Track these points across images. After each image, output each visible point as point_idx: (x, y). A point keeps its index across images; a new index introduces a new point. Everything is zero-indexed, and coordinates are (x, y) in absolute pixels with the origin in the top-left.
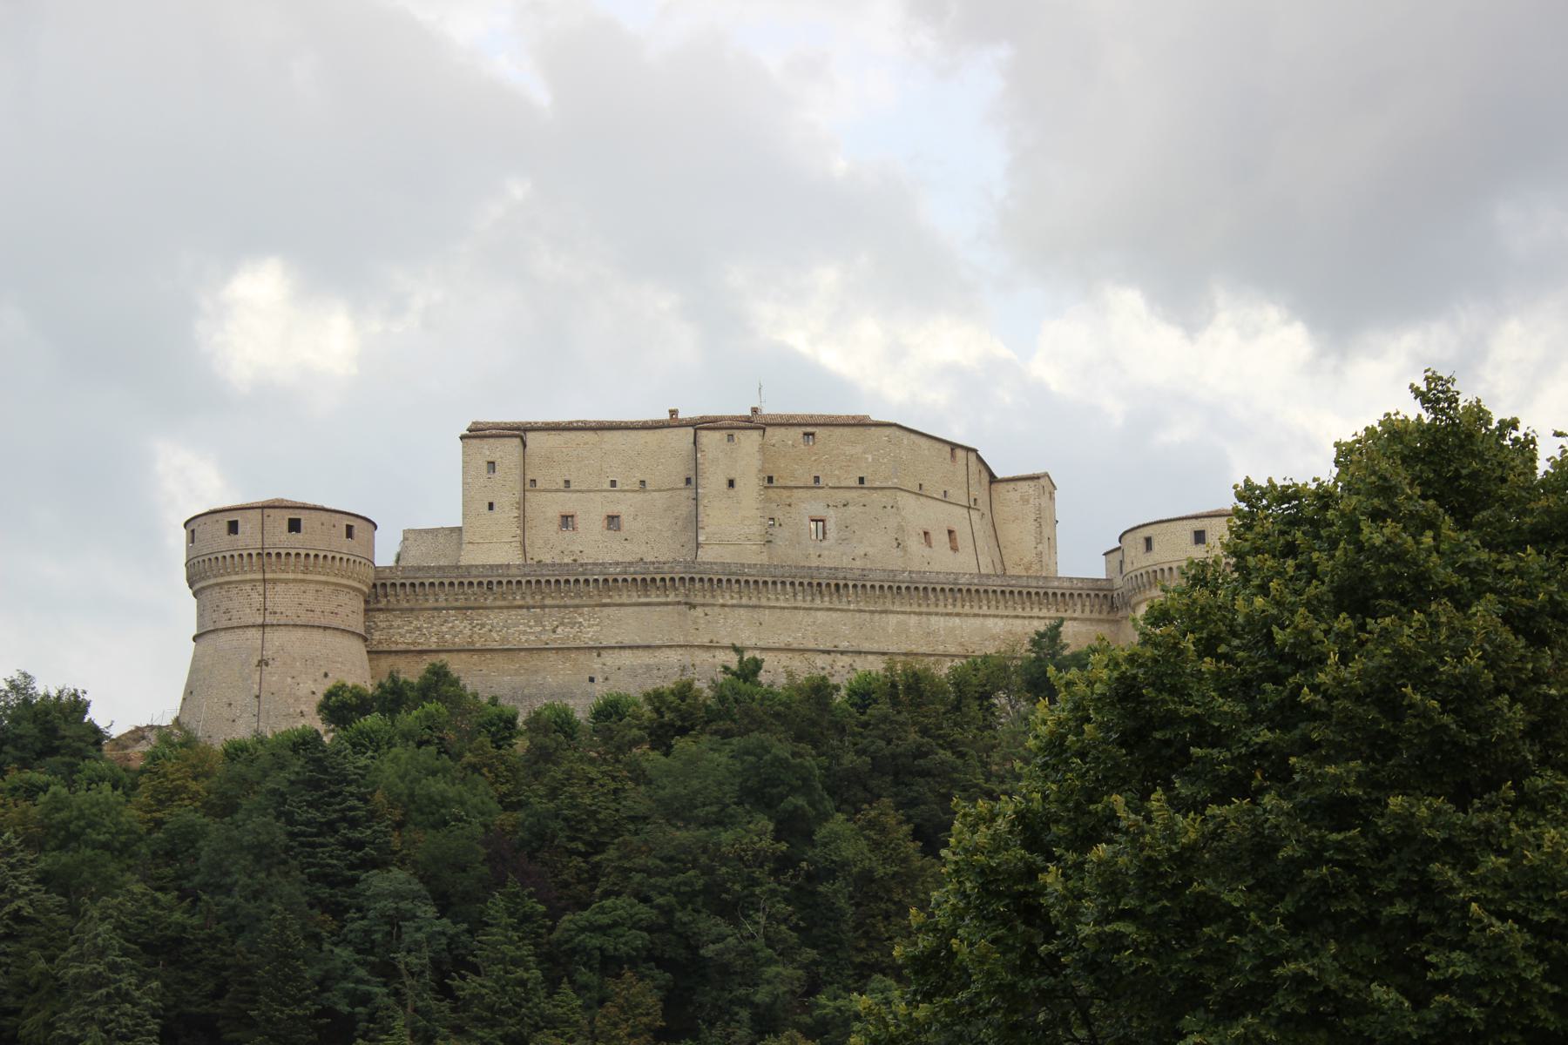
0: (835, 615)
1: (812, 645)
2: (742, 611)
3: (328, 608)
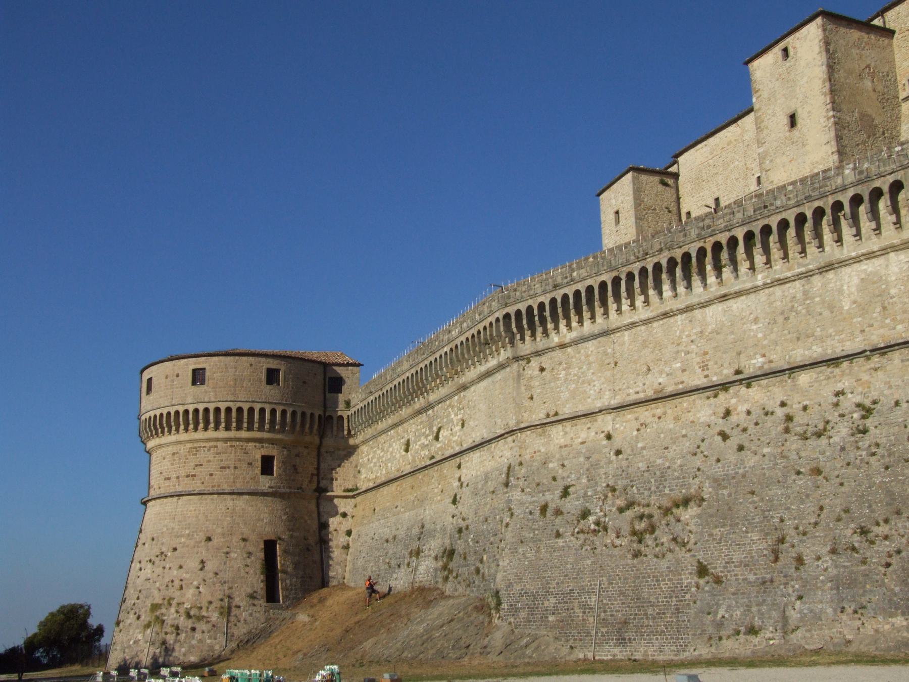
0: (735, 305)
1: (699, 380)
2: (591, 346)
3: (183, 473)
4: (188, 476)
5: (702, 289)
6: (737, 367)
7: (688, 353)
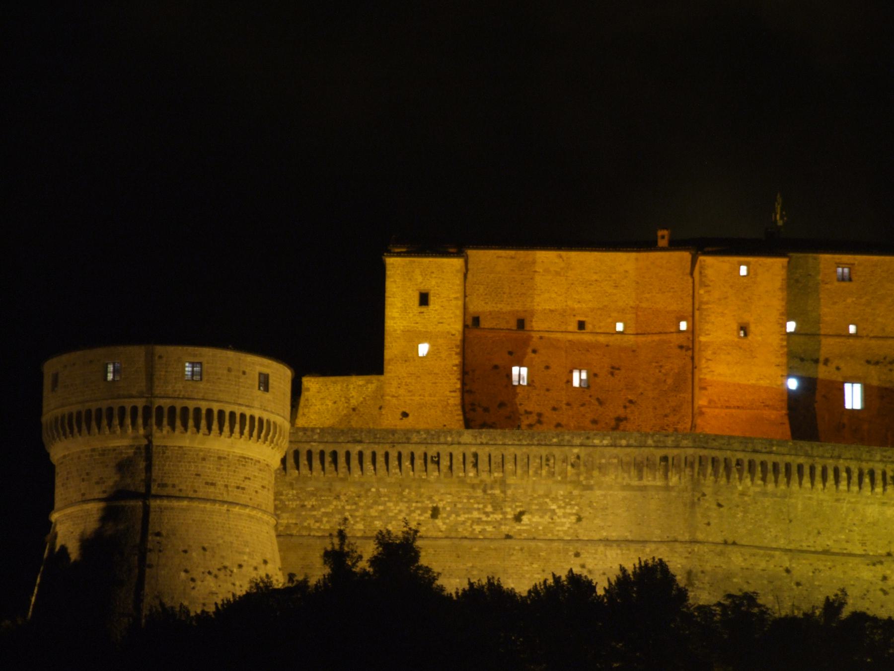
1: (858, 550)
2: (767, 501)
4: (238, 488)
5: (869, 494)
6: (888, 551)
7: (851, 531)
